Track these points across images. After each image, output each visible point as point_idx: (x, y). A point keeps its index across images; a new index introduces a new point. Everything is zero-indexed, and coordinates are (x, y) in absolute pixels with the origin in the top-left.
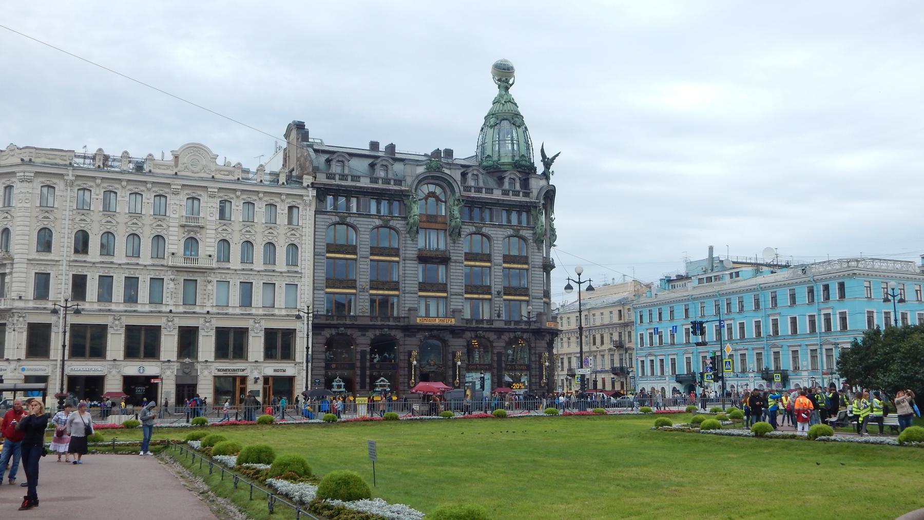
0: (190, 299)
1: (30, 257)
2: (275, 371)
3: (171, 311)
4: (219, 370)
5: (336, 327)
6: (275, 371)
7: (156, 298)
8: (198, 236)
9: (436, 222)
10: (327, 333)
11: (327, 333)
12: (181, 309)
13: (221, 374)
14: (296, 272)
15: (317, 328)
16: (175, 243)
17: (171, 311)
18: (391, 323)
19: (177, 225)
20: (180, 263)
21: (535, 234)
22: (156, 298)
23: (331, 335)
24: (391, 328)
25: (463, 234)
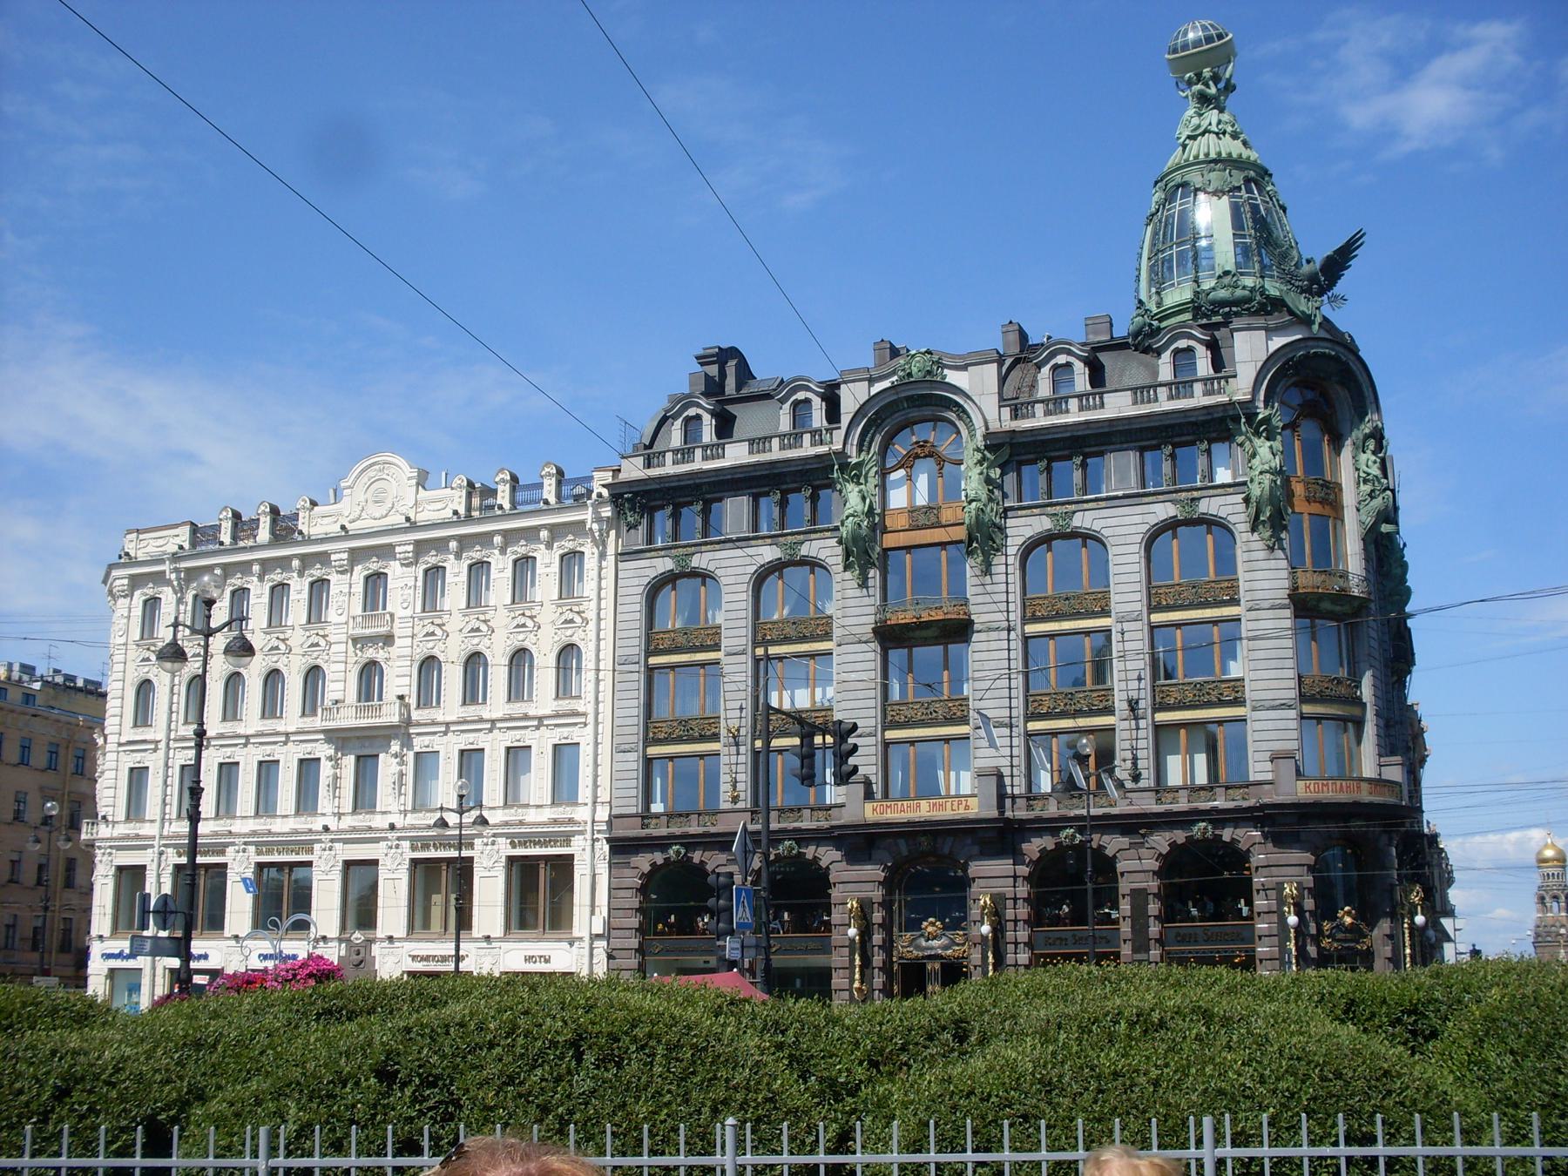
0: (364, 798)
1: (123, 740)
2: (529, 959)
3: (392, 827)
4: (414, 958)
5: (660, 844)
6: (529, 959)
7: (306, 800)
8: (380, 655)
9: (938, 525)
10: (644, 862)
11: (644, 862)
12: (348, 822)
13: (419, 967)
14: (575, 714)
15: (621, 848)
16: (341, 684)
17: (326, 829)
18: (805, 824)
19: (343, 638)
20: (348, 719)
21: (1247, 500)
22: (306, 800)
23: (653, 865)
24: (803, 838)
25: (1014, 544)
